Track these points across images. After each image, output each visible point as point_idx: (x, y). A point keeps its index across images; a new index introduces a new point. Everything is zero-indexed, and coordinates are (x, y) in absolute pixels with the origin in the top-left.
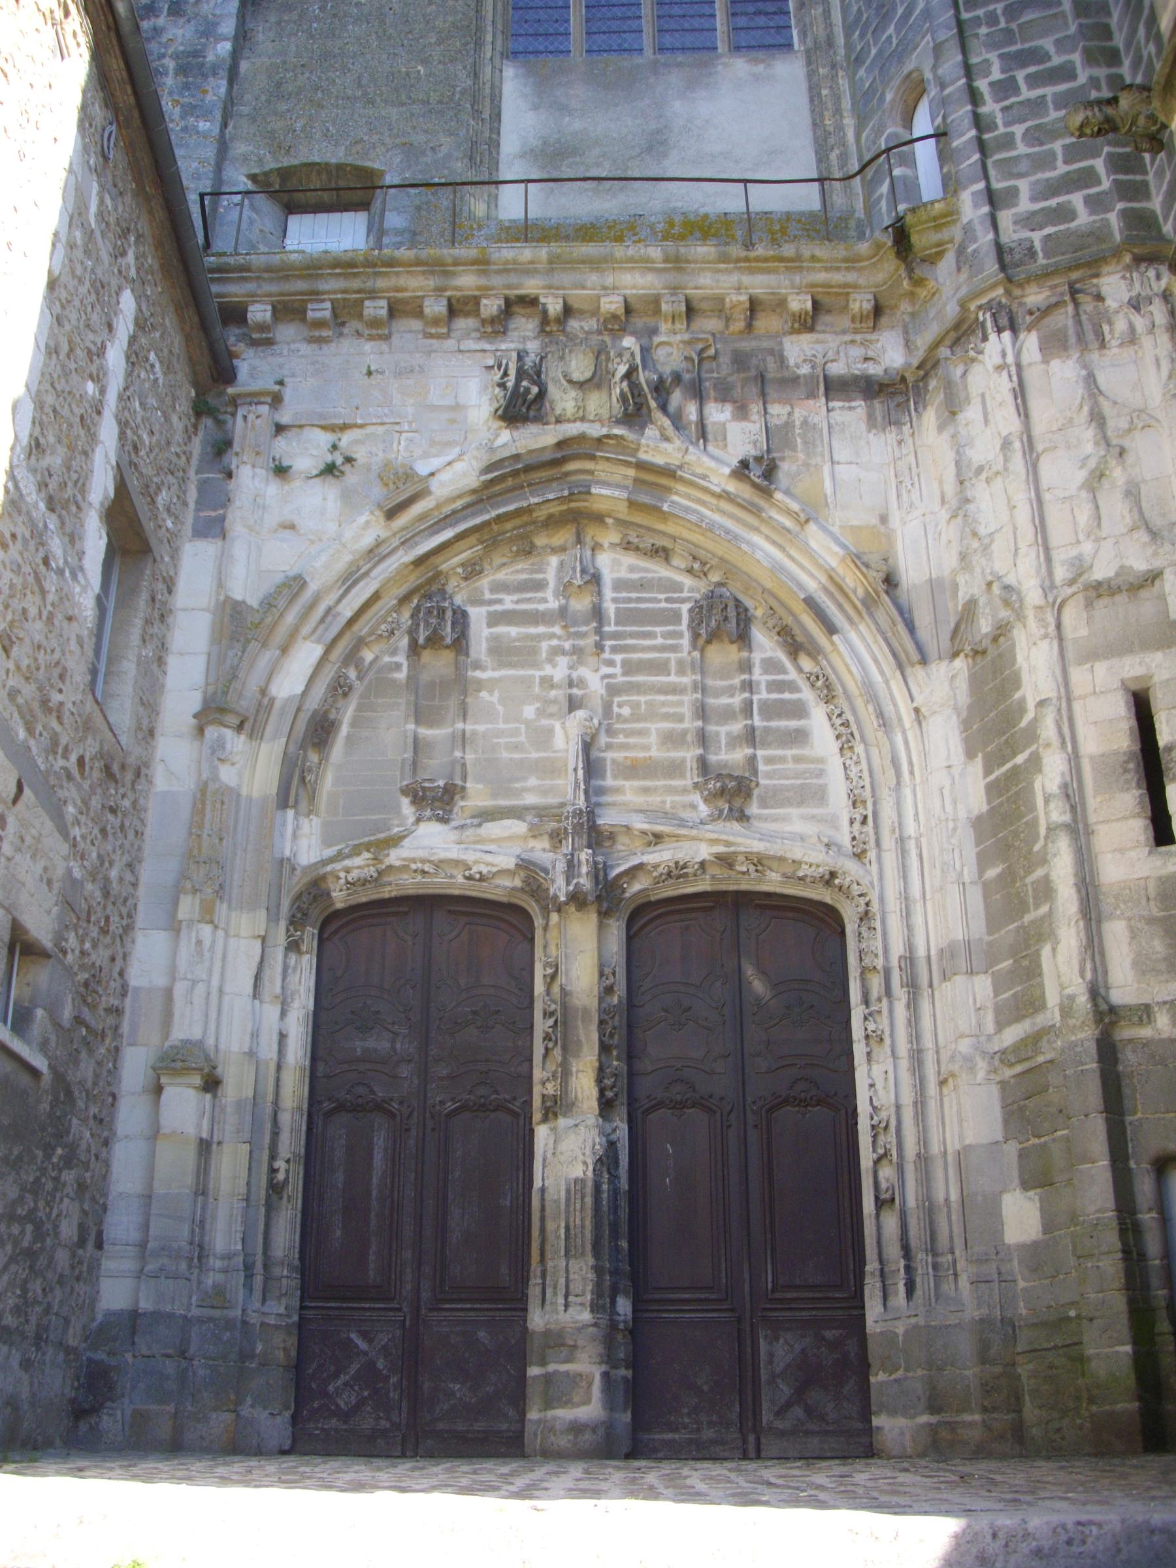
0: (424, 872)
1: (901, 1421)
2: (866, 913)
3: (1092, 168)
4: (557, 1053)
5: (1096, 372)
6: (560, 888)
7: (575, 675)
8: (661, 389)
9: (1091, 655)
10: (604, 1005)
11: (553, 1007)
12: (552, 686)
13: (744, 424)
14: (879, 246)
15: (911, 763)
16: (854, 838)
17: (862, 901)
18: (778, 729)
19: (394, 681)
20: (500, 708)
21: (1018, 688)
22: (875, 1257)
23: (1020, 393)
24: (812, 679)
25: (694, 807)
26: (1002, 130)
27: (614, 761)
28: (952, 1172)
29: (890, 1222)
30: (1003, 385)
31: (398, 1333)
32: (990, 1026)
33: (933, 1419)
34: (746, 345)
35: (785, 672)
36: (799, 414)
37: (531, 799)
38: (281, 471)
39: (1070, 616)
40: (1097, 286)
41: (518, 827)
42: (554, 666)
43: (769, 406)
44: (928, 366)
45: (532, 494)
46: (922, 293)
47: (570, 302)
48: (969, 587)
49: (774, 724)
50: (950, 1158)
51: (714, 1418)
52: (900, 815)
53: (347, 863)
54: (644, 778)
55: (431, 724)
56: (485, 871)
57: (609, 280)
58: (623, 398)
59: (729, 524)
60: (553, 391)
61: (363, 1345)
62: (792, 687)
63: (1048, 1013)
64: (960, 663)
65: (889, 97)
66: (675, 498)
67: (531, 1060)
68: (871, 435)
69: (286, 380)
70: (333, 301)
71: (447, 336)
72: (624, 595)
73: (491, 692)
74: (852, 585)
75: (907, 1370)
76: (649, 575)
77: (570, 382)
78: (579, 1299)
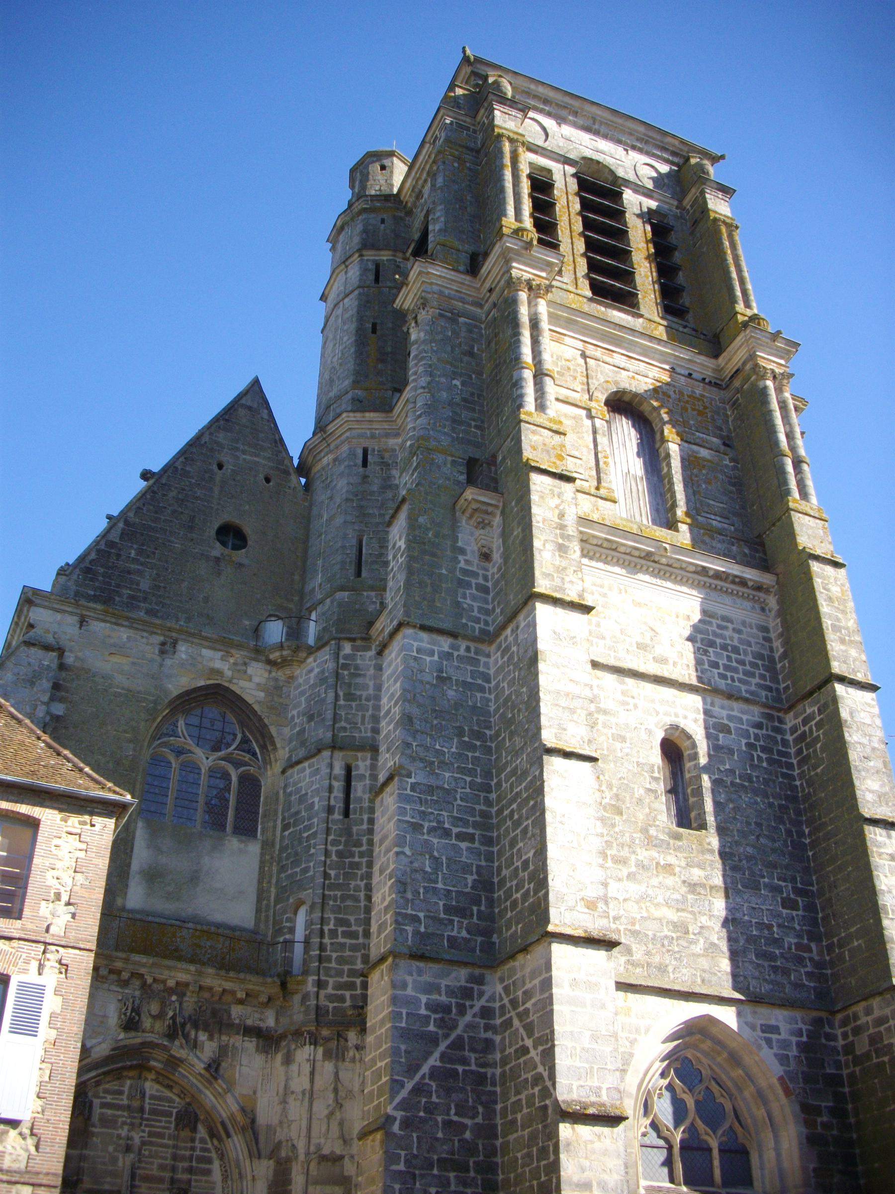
8: (183, 1025)
9: (316, 1183)
12: (121, 1138)
14: (274, 982)
20: (100, 1146)
23: (312, 1073)
26: (328, 953)
30: (307, 1068)
34: (217, 1006)
36: (232, 1041)
39: (313, 1165)
48: (280, 1135)
49: (200, 1165)
57: (172, 974)
58: (169, 1026)
59: (199, 1085)
64: (271, 1162)
65: (291, 900)
66: (180, 1069)
72: (153, 1102)
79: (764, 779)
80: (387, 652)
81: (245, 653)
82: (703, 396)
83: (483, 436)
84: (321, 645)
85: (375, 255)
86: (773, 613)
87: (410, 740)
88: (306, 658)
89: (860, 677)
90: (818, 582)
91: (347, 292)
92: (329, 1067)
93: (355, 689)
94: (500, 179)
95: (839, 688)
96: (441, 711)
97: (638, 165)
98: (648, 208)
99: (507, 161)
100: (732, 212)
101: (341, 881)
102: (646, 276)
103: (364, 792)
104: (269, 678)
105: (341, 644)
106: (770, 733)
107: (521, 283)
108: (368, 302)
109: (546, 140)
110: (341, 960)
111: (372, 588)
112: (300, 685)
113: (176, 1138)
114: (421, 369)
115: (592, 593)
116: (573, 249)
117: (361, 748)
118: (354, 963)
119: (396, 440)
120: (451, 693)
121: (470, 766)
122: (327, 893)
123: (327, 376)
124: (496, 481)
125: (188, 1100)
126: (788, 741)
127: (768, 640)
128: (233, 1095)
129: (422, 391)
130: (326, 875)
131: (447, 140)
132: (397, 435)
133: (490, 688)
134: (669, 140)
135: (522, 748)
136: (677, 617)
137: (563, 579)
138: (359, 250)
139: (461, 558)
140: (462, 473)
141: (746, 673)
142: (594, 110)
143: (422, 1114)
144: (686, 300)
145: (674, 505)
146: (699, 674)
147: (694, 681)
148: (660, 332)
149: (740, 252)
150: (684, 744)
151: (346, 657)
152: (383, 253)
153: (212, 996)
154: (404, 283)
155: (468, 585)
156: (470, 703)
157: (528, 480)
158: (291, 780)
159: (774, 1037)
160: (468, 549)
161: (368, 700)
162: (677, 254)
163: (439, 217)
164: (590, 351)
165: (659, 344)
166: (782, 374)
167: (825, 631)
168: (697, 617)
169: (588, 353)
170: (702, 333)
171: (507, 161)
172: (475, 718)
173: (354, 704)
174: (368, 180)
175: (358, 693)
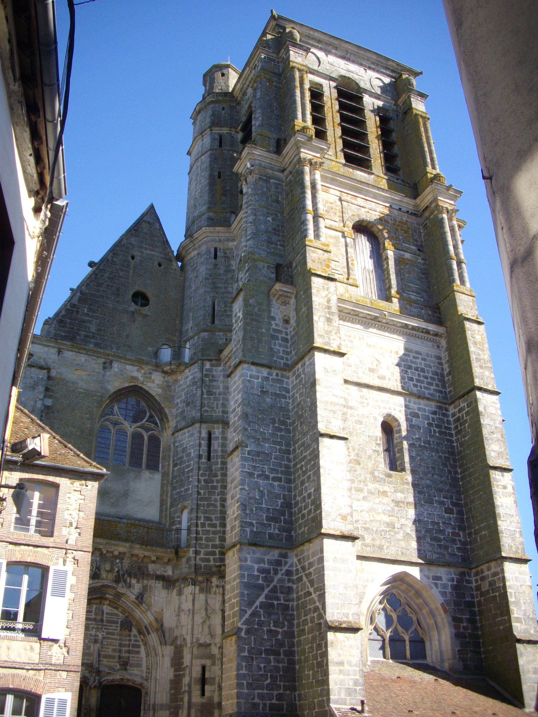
8: (123, 575)
9: (197, 658)
14: (172, 551)
23: (193, 600)
24: (143, 640)
25: (116, 666)
26: (201, 535)
30: (190, 598)
34: (141, 565)
48: (177, 633)
57: (117, 548)
58: (116, 576)
60: (102, 572)
62: (138, 641)
64: (172, 647)
65: (179, 506)
77: (106, 570)
79: (437, 442)
80: (233, 375)
81: (150, 367)
82: (406, 221)
83: (284, 250)
84: (192, 362)
85: (219, 130)
86: (444, 349)
87: (247, 426)
88: (184, 370)
89: (490, 387)
90: (469, 334)
91: (203, 152)
92: (202, 597)
93: (212, 389)
94: (293, 95)
95: (479, 394)
96: (263, 410)
97: (372, 79)
98: (378, 107)
99: (297, 84)
100: (426, 109)
101: (207, 496)
102: (376, 149)
103: (218, 446)
104: (164, 381)
105: (205, 362)
106: (441, 417)
107: (305, 161)
108: (216, 159)
109: (319, 66)
110: (207, 539)
111: (220, 330)
112: (181, 385)
113: (120, 635)
114: (249, 212)
115: (344, 340)
116: (334, 134)
117: (217, 422)
118: (215, 541)
119: (233, 243)
120: (268, 400)
121: (279, 440)
122: (199, 503)
123: (192, 202)
124: (291, 277)
125: (126, 615)
126: (450, 421)
127: (440, 364)
128: (151, 612)
129: (250, 224)
130: (199, 493)
131: (263, 69)
132: (233, 240)
133: (289, 396)
134: (390, 63)
135: (307, 432)
136: (391, 352)
137: (329, 337)
138: (210, 127)
139: (273, 322)
140: (273, 273)
141: (428, 384)
142: (347, 46)
143: (256, 626)
144: (398, 162)
145: (390, 287)
146: (403, 385)
147: (400, 389)
148: (384, 184)
149: (430, 134)
150: (394, 424)
151: (207, 370)
152: (223, 129)
153: (138, 559)
154: (238, 159)
155: (277, 338)
156: (279, 405)
157: (310, 281)
158: (178, 439)
159: (439, 582)
160: (277, 317)
161: (220, 394)
162: (394, 134)
163: (258, 117)
164: (344, 197)
165: (383, 192)
166: (452, 210)
167: (472, 362)
168: (402, 352)
169: (343, 198)
170: (407, 183)
171: (297, 84)
172: (281, 413)
173: (212, 397)
174: (214, 83)
175: (214, 391)
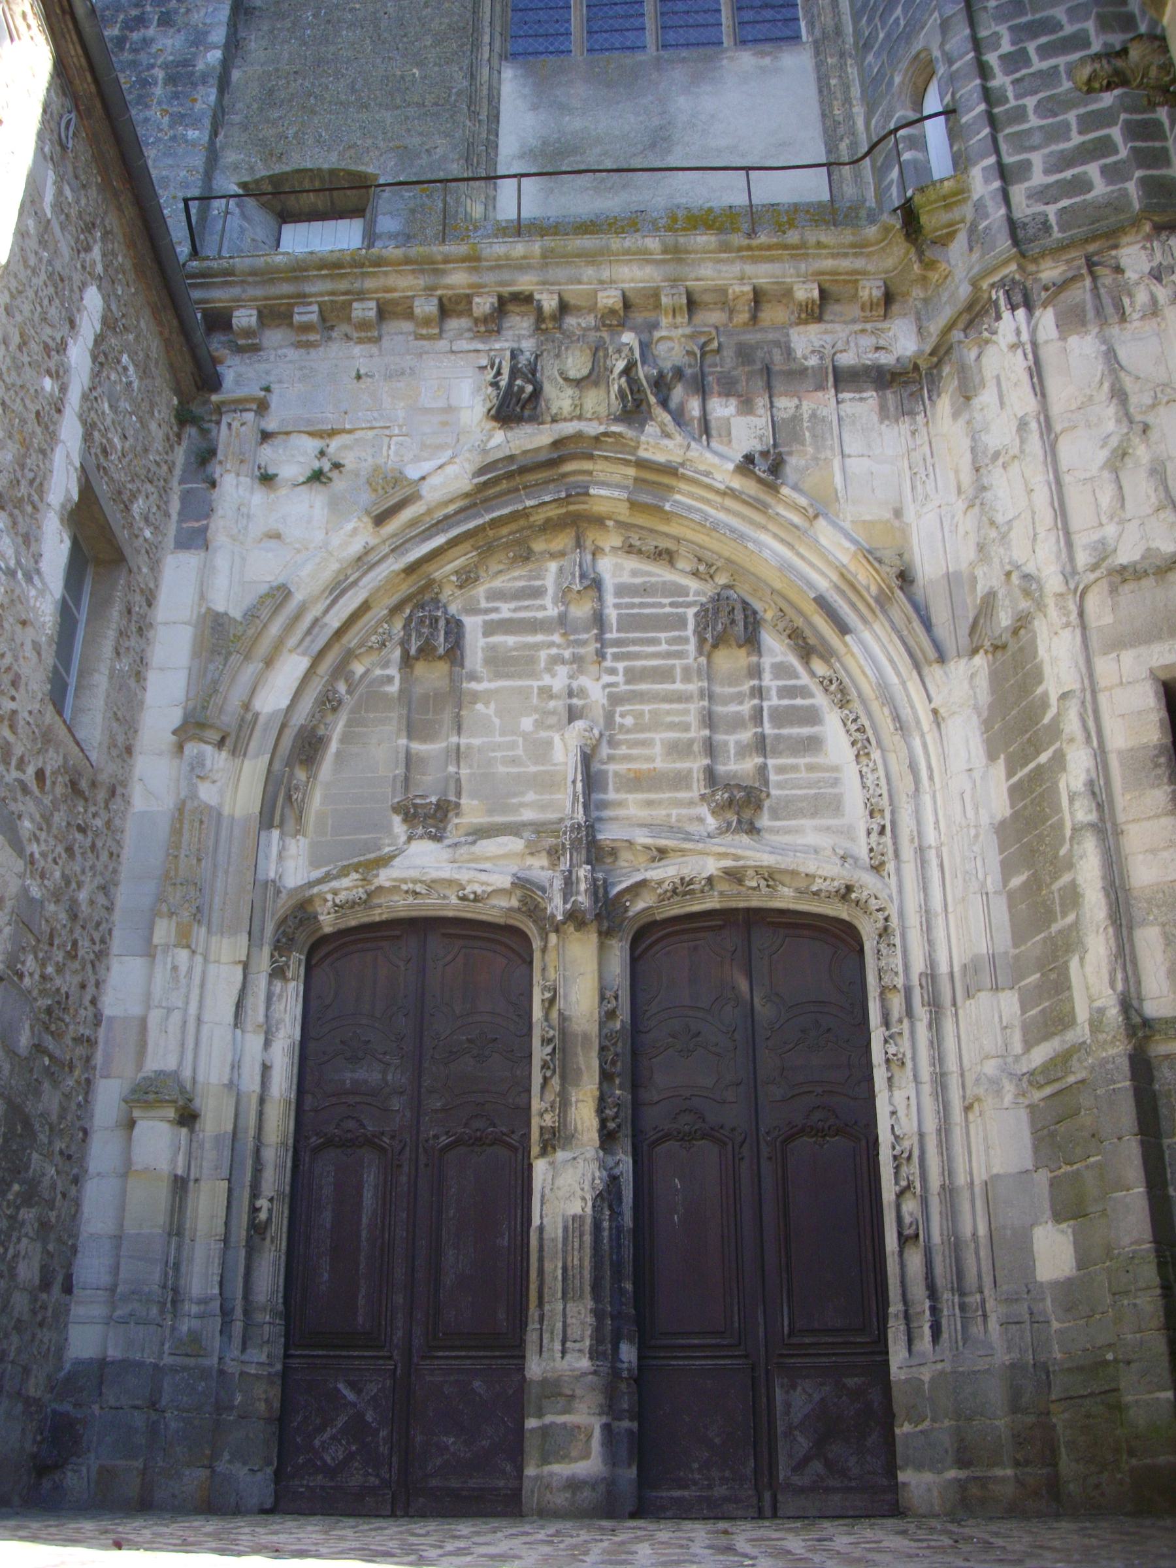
0: (415, 893)
1: (928, 1477)
2: (886, 929)
3: (1108, 137)
4: (555, 1082)
5: (1117, 347)
6: (557, 907)
7: (575, 684)
8: (661, 385)
9: (1117, 644)
10: (605, 1031)
11: (551, 1033)
12: (551, 697)
13: (750, 418)
14: (887, 230)
15: (930, 768)
16: (871, 850)
17: (881, 916)
18: (790, 737)
19: (386, 694)
20: (497, 721)
21: (1040, 682)
22: (899, 1297)
23: (1037, 372)
24: (825, 684)
25: (701, 820)
26: (1013, 103)
27: (616, 774)
28: (979, 1204)
29: (915, 1260)
30: (1018, 364)
31: (388, 1383)
32: (1017, 1047)
33: (962, 1474)
34: (751, 337)
35: (797, 677)
36: (807, 407)
37: (528, 815)
38: (267, 479)
39: (1093, 602)
40: (1115, 257)
41: (514, 844)
42: (553, 676)
43: (775, 400)
44: (942, 352)
45: (528, 497)
46: (934, 276)
47: (567, 297)
48: (988, 579)
49: (785, 731)
50: (978, 1189)
51: (727, 1474)
52: (919, 823)
53: (335, 884)
54: (649, 791)
55: (424, 739)
56: (479, 891)
57: (606, 274)
58: (622, 395)
59: (735, 522)
60: (549, 390)
61: (351, 1396)
62: (804, 692)
63: (1078, 1029)
64: (979, 660)
65: (897, 79)
66: (678, 497)
67: (529, 1091)
68: (883, 427)
69: (273, 386)
70: (320, 304)
71: (440, 336)
73: (487, 704)
74: (864, 582)
75: (933, 1420)
76: (653, 579)
77: (566, 379)
78: (577, 1346)
